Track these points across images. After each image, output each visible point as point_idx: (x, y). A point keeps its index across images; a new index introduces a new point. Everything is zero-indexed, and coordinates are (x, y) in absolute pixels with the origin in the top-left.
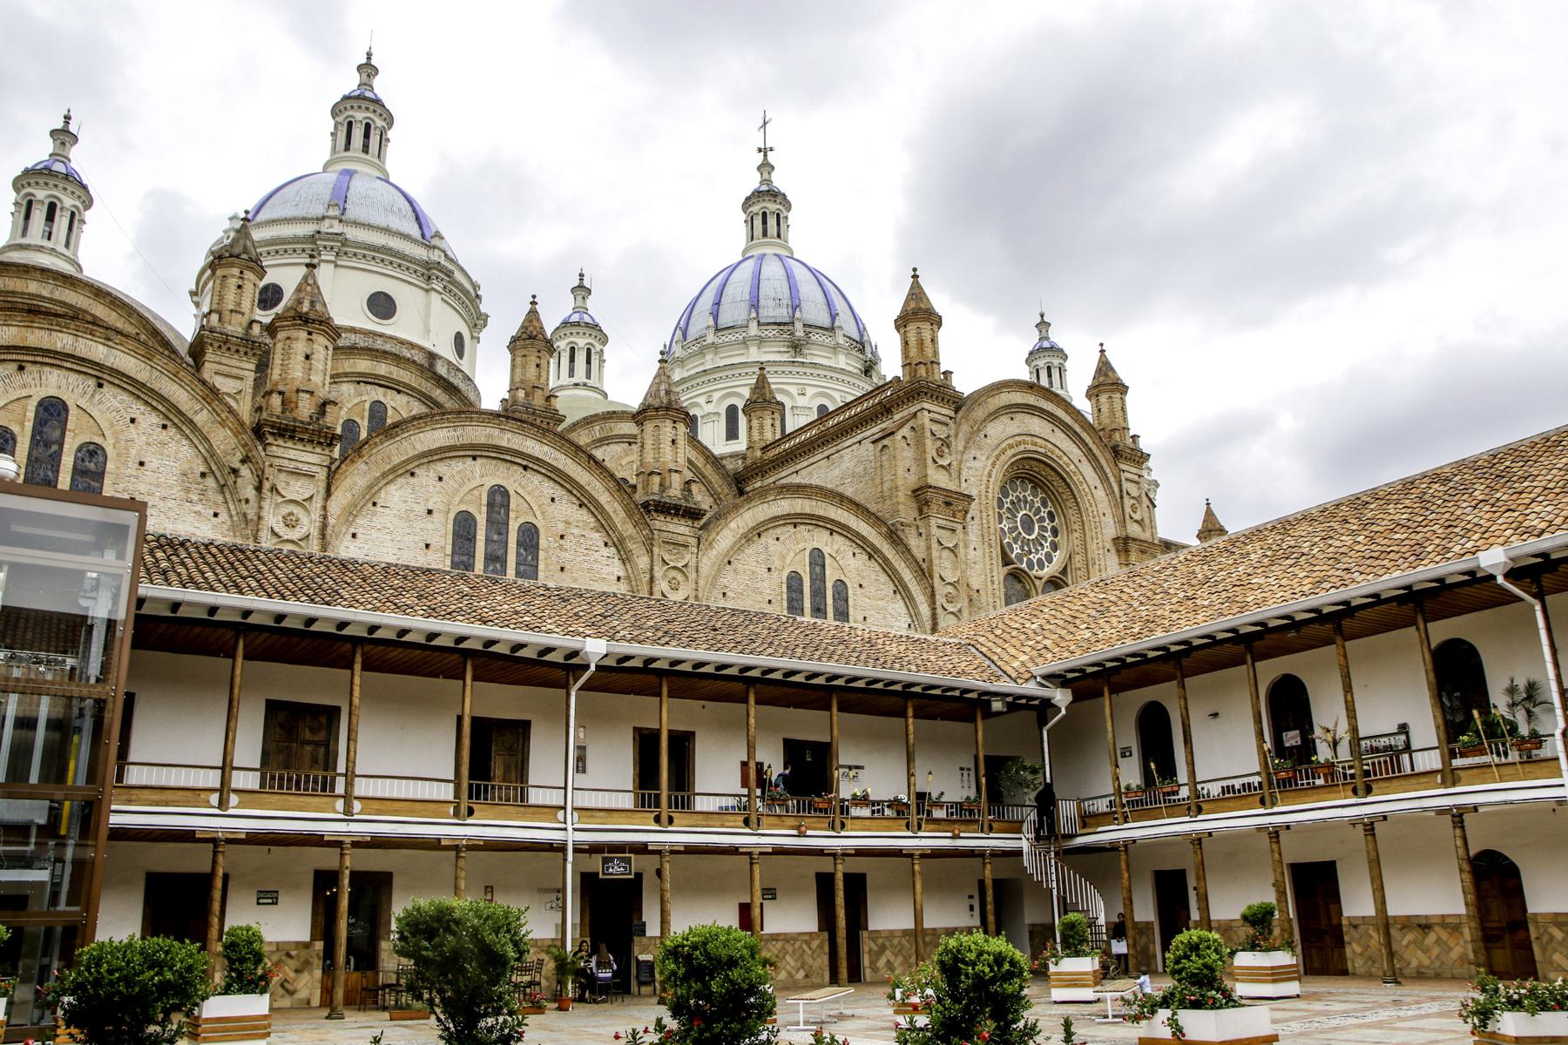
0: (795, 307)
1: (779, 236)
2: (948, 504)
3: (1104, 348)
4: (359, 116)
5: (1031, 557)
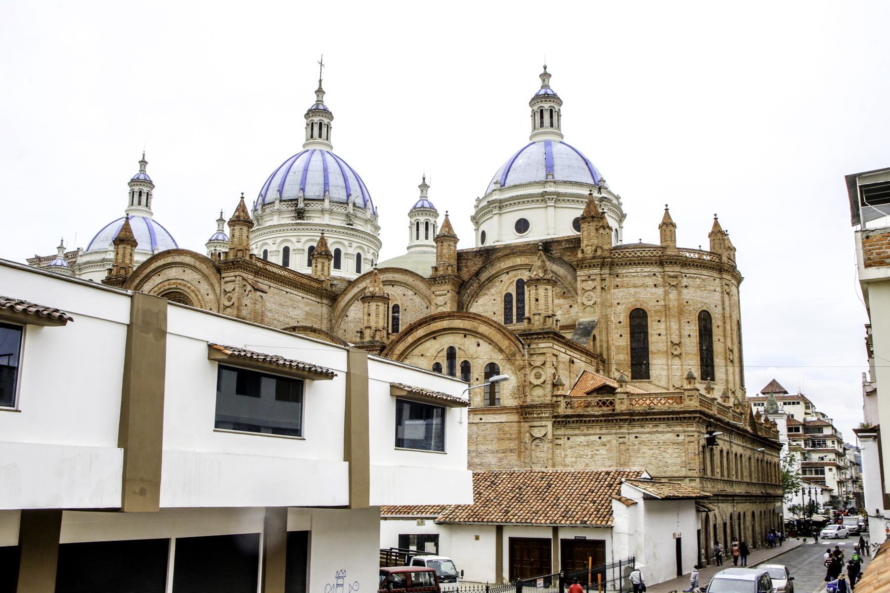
3: (244, 196)
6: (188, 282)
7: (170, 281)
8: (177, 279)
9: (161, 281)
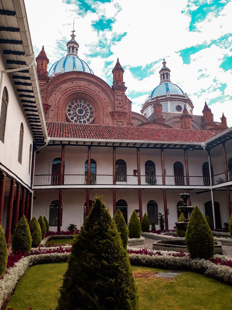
5: (81, 120)
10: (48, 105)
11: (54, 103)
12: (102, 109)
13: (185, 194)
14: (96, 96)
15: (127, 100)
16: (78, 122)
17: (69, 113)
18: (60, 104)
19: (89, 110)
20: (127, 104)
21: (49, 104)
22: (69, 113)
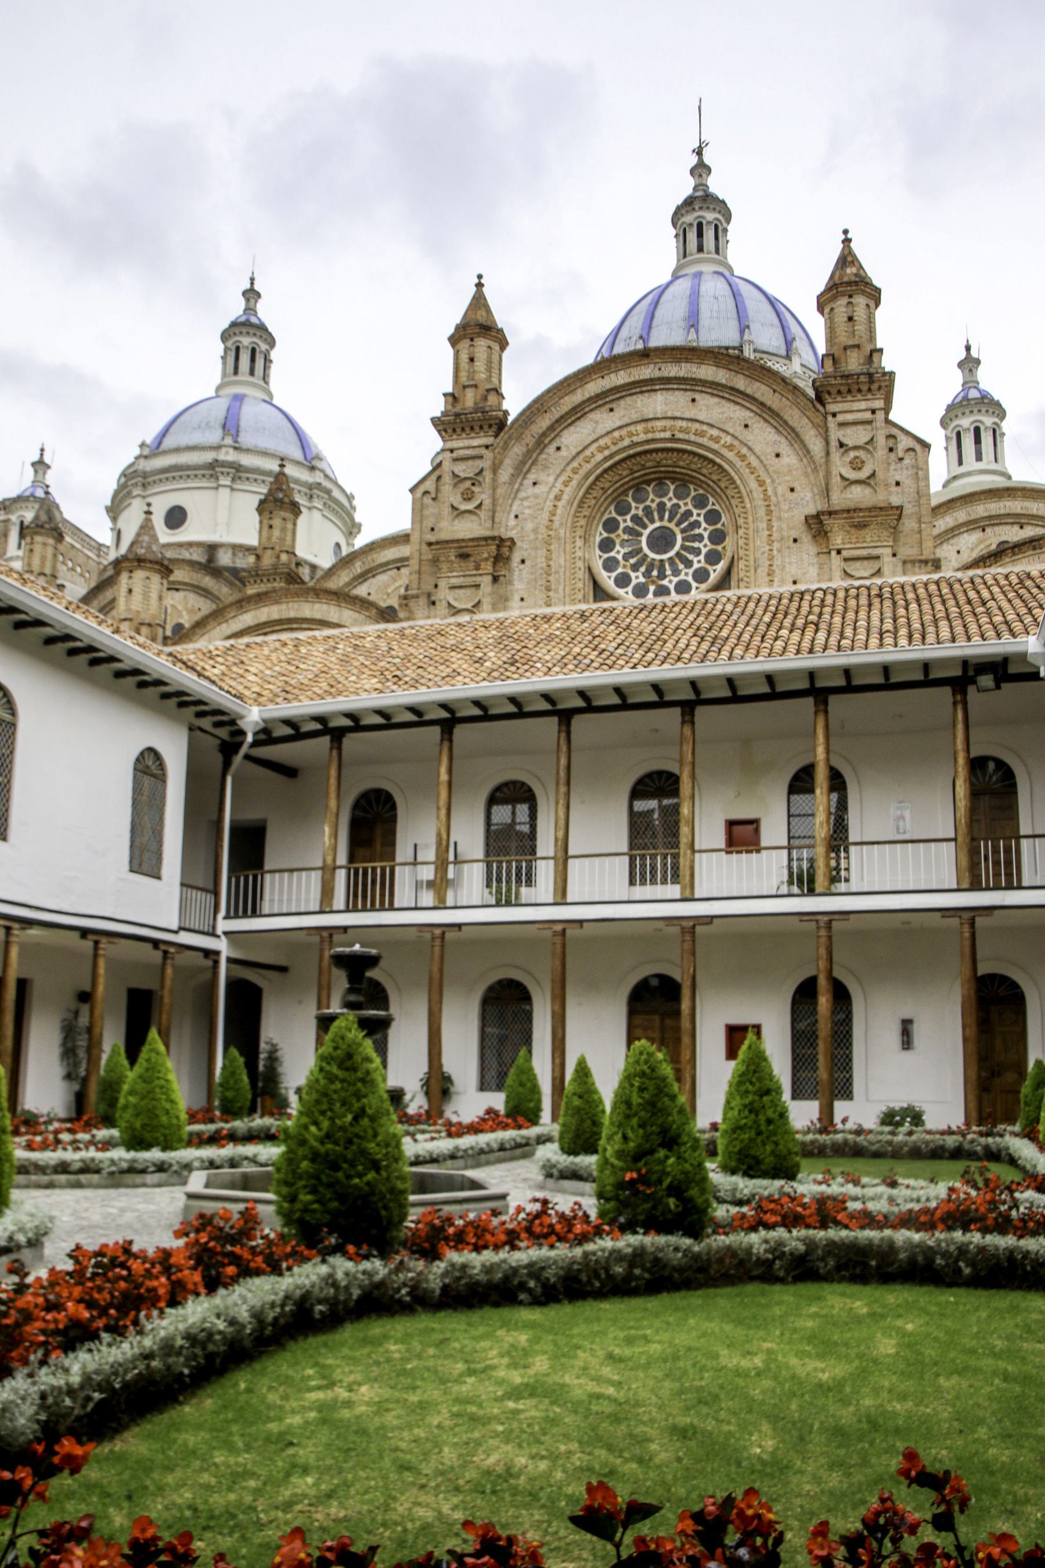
0: (744, 328)
1: (717, 252)
2: (464, 556)
4: (246, 341)
5: (665, 582)
6: (712, 426)
7: (650, 425)
8: (674, 418)
9: (618, 424)
10: (502, 540)
11: (529, 526)
12: (762, 512)
13: (357, 947)
14: (730, 447)
15: (901, 436)
16: (650, 595)
17: (606, 556)
18: (556, 524)
19: (704, 525)
20: (901, 459)
21: (506, 534)
22: (606, 556)
